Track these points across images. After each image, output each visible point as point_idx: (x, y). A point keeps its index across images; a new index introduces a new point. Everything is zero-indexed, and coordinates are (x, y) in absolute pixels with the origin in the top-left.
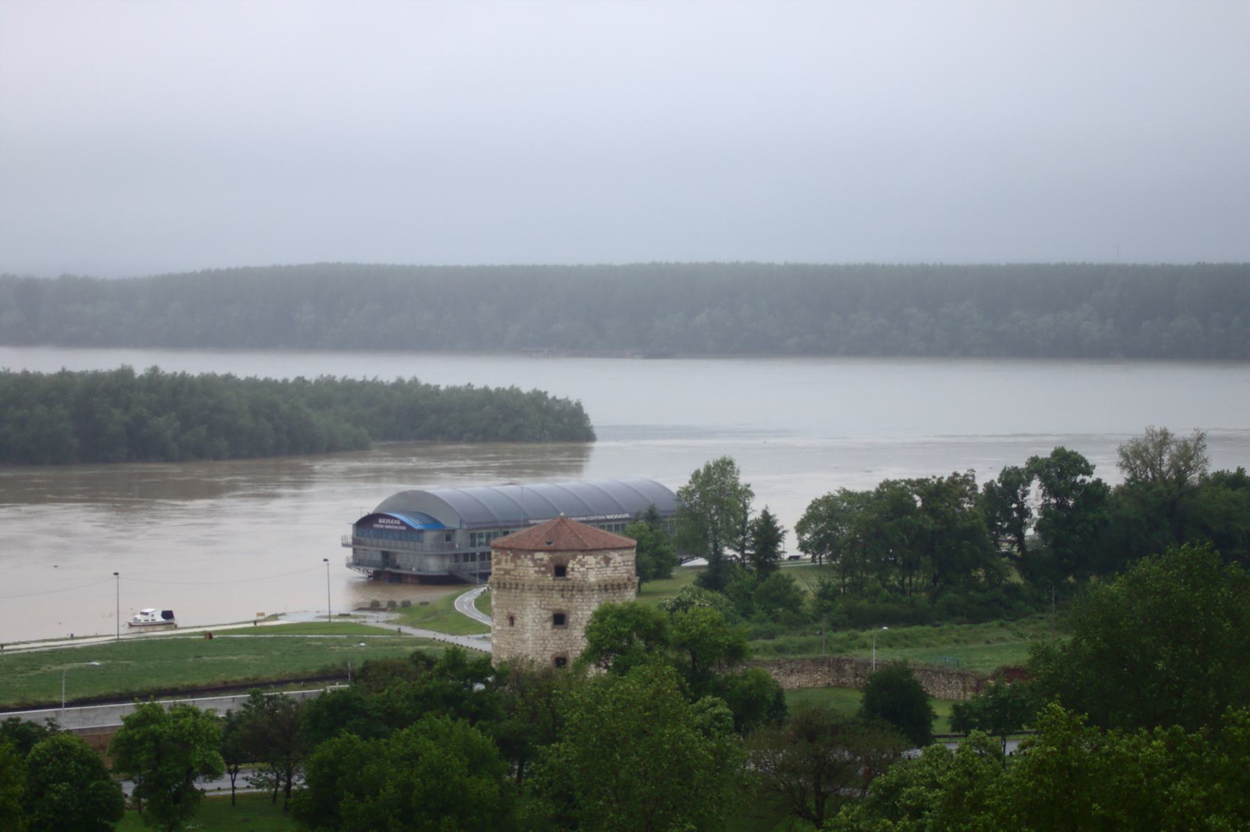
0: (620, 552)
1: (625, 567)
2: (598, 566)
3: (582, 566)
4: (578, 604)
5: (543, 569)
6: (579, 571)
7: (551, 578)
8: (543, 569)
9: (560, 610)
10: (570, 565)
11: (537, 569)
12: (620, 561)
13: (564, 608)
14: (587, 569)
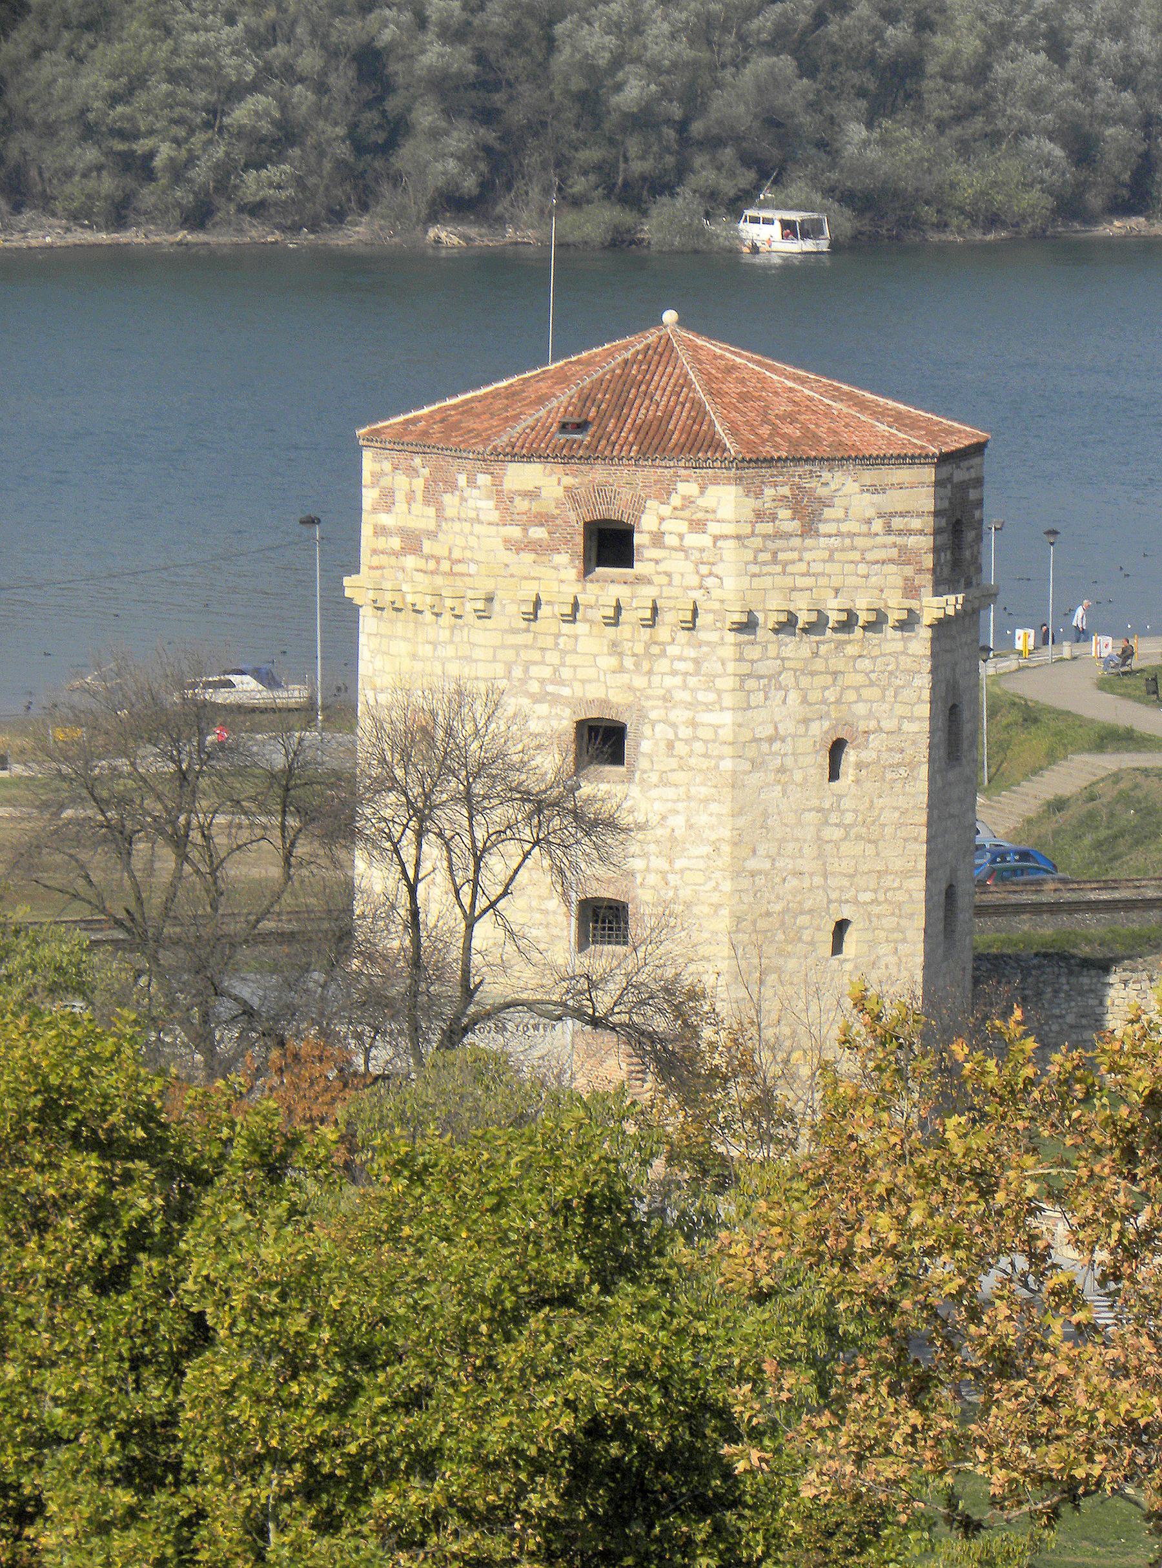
0: (869, 476)
1: (891, 539)
3: (698, 526)
4: (678, 680)
5: (538, 533)
6: (681, 549)
9: (605, 703)
11: (515, 532)
12: (871, 513)
13: (618, 697)
14: (716, 538)
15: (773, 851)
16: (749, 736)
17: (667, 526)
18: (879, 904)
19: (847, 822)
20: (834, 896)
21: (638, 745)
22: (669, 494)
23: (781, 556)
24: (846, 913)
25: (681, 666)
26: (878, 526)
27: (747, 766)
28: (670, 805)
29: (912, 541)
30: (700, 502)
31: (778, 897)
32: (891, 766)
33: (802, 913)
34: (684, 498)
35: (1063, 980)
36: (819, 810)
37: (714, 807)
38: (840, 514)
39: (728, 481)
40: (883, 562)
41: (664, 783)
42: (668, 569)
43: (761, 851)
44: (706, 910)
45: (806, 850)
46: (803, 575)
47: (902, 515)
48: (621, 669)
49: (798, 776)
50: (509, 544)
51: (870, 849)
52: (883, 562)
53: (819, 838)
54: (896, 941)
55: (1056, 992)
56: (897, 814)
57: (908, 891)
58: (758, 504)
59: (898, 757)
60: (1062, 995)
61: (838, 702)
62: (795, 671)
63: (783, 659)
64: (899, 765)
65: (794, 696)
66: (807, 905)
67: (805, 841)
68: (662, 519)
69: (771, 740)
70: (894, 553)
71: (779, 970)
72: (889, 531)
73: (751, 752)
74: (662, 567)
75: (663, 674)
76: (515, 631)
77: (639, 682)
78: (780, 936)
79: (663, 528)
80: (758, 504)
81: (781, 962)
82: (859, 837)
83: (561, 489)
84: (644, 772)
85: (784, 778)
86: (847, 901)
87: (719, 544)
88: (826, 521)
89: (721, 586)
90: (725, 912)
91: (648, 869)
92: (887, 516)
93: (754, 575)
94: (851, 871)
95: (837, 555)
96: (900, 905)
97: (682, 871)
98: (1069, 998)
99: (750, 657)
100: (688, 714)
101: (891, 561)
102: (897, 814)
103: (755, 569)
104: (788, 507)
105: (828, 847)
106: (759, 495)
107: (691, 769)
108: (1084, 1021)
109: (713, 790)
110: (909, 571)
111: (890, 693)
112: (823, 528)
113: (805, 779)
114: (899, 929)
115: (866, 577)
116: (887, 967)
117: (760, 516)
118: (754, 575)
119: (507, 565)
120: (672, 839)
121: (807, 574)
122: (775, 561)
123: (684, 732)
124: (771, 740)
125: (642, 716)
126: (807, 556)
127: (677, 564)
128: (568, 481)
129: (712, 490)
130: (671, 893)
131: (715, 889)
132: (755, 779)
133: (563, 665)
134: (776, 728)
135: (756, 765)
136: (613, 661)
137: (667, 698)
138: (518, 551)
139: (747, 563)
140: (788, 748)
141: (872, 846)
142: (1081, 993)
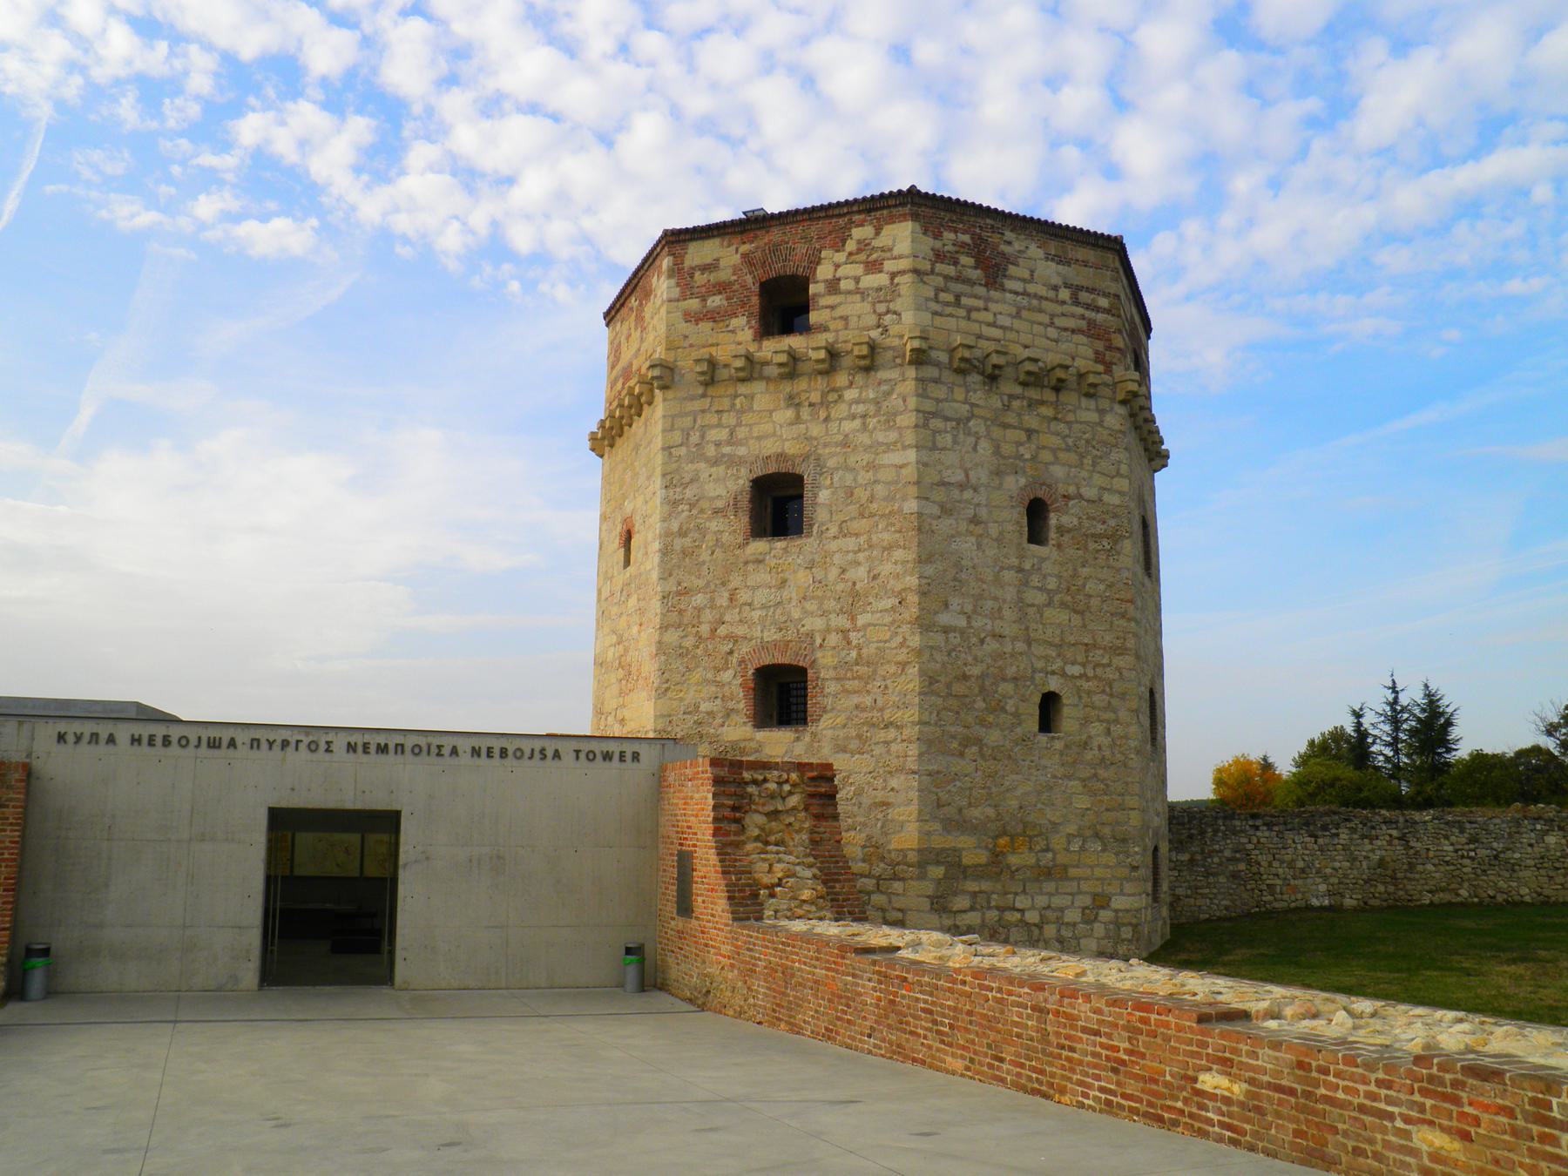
0: (1053, 247)
1: (1079, 310)
2: (950, 270)
3: (874, 267)
4: (857, 423)
5: (716, 301)
6: (858, 291)
7: (747, 335)
8: (716, 301)
9: (781, 457)
10: (824, 271)
11: (694, 304)
12: (1056, 280)
13: (791, 448)
14: (893, 275)
15: (969, 608)
16: (937, 479)
17: (841, 272)
18: (1088, 679)
19: (1050, 587)
21: (815, 496)
22: (844, 241)
23: (964, 301)
24: (1054, 685)
25: (860, 409)
26: (1065, 294)
27: (936, 510)
28: (850, 556)
29: (1100, 317)
30: (876, 243)
31: (975, 659)
32: (1093, 535)
33: (1004, 680)
34: (859, 242)
35: (1220, 822)
36: (1020, 570)
37: (898, 554)
38: (1026, 275)
39: (903, 218)
40: (1073, 331)
41: (843, 533)
42: (842, 314)
43: (955, 602)
44: (893, 669)
45: (1007, 613)
46: (989, 325)
47: (1088, 290)
48: (797, 420)
49: (994, 530)
50: (689, 317)
52: (1073, 331)
53: (1021, 600)
54: (1108, 722)
55: (1216, 831)
56: (1102, 587)
57: (1119, 669)
58: (938, 244)
59: (1100, 528)
60: (1220, 834)
61: (1034, 458)
62: (986, 419)
63: (972, 405)
64: (1101, 536)
65: (985, 447)
66: (1011, 671)
67: (1004, 601)
68: (837, 266)
69: (962, 487)
70: (1083, 324)
71: (979, 741)
72: (1076, 302)
73: (939, 495)
74: (839, 312)
75: (842, 419)
76: (693, 398)
77: (816, 430)
78: (980, 704)
79: (837, 276)
80: (938, 244)
81: (981, 731)
82: (1063, 605)
83: (738, 256)
84: (822, 524)
85: (979, 530)
86: (1053, 673)
87: (896, 280)
88: (1011, 278)
89: (899, 322)
90: (913, 670)
91: (828, 630)
92: (1076, 290)
93: (935, 313)
94: (1057, 640)
95: (1024, 314)
96: (1110, 684)
97: (866, 626)
98: (1225, 837)
99: (935, 395)
100: (867, 457)
102: (1102, 587)
103: (935, 306)
104: (968, 254)
105: (1031, 611)
106: (937, 236)
107: (872, 515)
108: (1238, 855)
109: (897, 535)
110: (1100, 345)
111: (1088, 461)
112: (1009, 284)
114: (1109, 707)
115: (1056, 341)
116: (1100, 748)
117: (939, 256)
118: (935, 313)
119: (686, 337)
120: (855, 595)
121: (993, 325)
123: (865, 476)
124: (962, 487)
125: (819, 463)
126: (993, 306)
127: (856, 308)
128: (745, 248)
130: (854, 654)
131: (902, 645)
132: (945, 525)
133: (739, 424)
134: (967, 476)
135: (946, 510)
136: (790, 413)
137: (845, 443)
138: (697, 321)
139: (927, 299)
140: (981, 498)
141: (1078, 617)
142: (1235, 833)
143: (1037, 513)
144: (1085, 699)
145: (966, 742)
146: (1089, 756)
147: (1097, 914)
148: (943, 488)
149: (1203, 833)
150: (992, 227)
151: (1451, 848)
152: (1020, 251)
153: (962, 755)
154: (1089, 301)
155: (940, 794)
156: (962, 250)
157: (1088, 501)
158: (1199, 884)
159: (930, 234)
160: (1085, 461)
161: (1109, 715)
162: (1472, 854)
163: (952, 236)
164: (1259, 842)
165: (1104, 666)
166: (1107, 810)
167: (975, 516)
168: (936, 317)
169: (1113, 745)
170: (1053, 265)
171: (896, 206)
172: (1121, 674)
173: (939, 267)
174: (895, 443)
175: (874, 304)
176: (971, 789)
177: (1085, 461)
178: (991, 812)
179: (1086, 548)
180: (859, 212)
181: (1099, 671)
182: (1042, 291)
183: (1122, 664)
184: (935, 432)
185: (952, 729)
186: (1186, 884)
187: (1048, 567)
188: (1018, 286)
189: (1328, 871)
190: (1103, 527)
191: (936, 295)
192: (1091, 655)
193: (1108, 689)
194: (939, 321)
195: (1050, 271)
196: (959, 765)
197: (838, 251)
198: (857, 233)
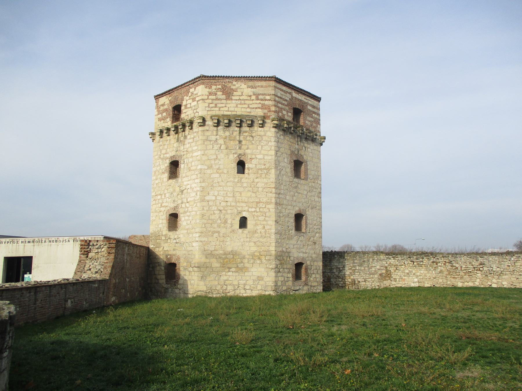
0: (251, 83)
1: (258, 102)
2: (214, 97)
3: (194, 100)
10: (184, 103)
11: (160, 116)
12: (251, 94)
14: (198, 101)
18: (257, 212)
20: (239, 209)
23: (219, 105)
24: (244, 214)
26: (254, 97)
29: (267, 103)
32: (260, 169)
43: (211, 193)
47: (262, 95)
51: (254, 195)
52: (256, 108)
55: (373, 260)
56: (263, 184)
57: (269, 209)
58: (210, 90)
59: (263, 167)
60: (375, 261)
64: (264, 169)
72: (258, 99)
80: (210, 90)
86: (244, 211)
92: (257, 95)
96: (265, 213)
101: (259, 108)
103: (209, 109)
106: (210, 88)
108: (382, 268)
111: (259, 147)
112: (233, 98)
113: (228, 172)
114: (265, 220)
115: (250, 112)
117: (210, 94)
122: (216, 106)
124: (215, 159)
126: (228, 106)
129: (197, 88)
132: (209, 171)
135: (210, 167)
141: (254, 194)
142: (381, 260)
143: (241, 165)
144: (256, 218)
145: (214, 232)
146: (256, 235)
147: (259, 282)
148: (208, 161)
149: (368, 261)
150: (229, 81)
151: (472, 267)
152: (238, 87)
153: (212, 236)
154: (263, 98)
155: (205, 247)
156: (218, 90)
157: (259, 159)
158: (367, 277)
159: (208, 88)
160: (258, 147)
161: (265, 223)
162: (481, 269)
163: (215, 87)
164: (390, 263)
165: (263, 208)
166: (263, 251)
167: (219, 167)
168: (208, 112)
169: (265, 232)
170: (250, 89)
171: (198, 81)
172: (269, 210)
173: (210, 97)
174: (196, 150)
175: (193, 110)
176: (215, 246)
177: (258, 147)
178: (221, 252)
179: (258, 173)
180: (191, 84)
181: (261, 210)
182: (246, 98)
183: (270, 207)
184: (206, 145)
185: (209, 229)
186: (362, 277)
187: (243, 180)
188: (237, 98)
189: (418, 274)
190: (264, 166)
191: (209, 105)
192: (258, 205)
193: (264, 215)
194: (209, 113)
195: (250, 91)
196: (210, 239)
197: (187, 96)
198: (192, 90)
